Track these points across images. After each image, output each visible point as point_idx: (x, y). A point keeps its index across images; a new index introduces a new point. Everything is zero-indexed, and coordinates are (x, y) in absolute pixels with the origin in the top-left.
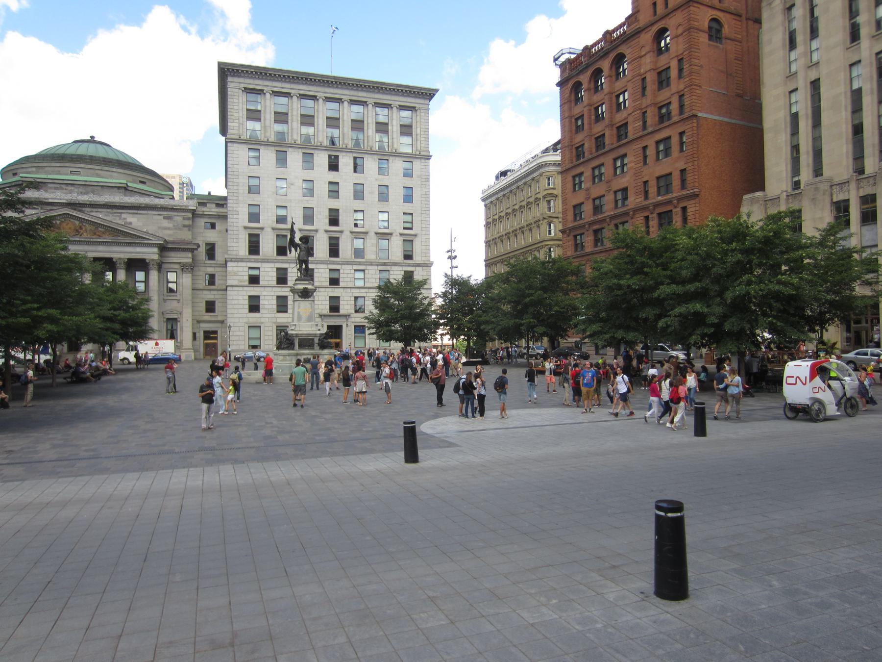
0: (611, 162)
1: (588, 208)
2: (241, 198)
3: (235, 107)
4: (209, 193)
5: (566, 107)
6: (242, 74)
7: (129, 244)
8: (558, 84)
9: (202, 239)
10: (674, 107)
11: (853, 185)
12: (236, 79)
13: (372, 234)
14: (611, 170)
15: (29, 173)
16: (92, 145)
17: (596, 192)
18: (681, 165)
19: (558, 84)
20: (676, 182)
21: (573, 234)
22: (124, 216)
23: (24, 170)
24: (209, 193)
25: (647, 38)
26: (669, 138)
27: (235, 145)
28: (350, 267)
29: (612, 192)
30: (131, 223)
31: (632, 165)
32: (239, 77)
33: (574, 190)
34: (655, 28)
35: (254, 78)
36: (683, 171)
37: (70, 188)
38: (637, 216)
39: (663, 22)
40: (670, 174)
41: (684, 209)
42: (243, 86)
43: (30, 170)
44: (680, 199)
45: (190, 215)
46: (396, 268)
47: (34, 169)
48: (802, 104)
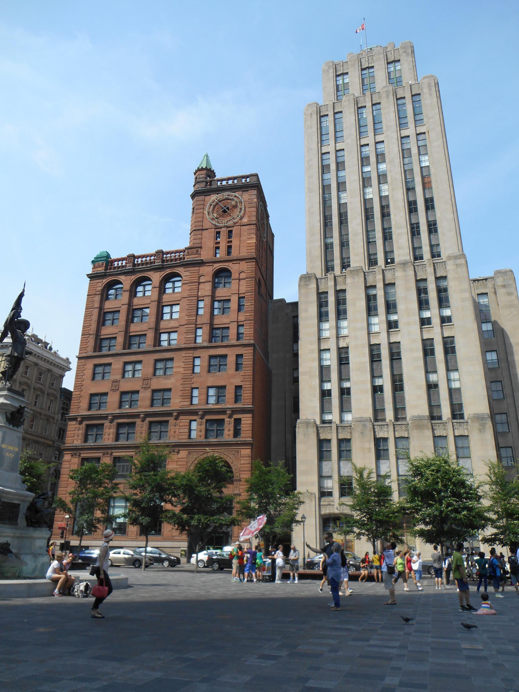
0: (152, 362)
1: (113, 399)
5: (97, 298)
8: (90, 276)
10: (233, 332)
11: (391, 428)
14: (151, 370)
17: (125, 386)
18: (238, 382)
19: (90, 276)
20: (230, 393)
21: (85, 423)
25: (208, 271)
26: (225, 356)
29: (150, 390)
31: (182, 370)
33: (93, 379)
34: (217, 266)
36: (238, 388)
38: (181, 417)
39: (227, 264)
40: (224, 387)
41: (238, 422)
44: (235, 411)
48: (331, 359)
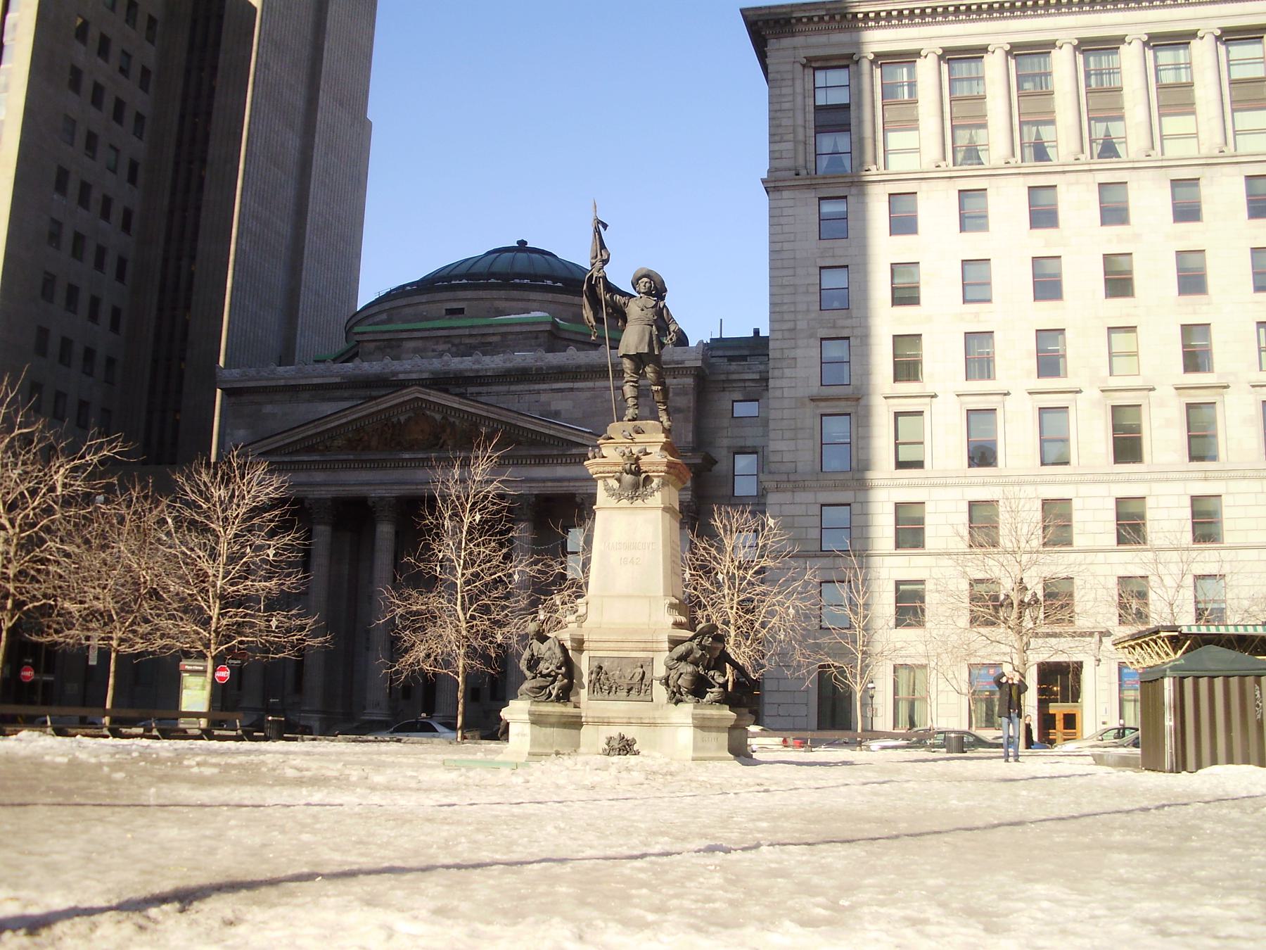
2: (801, 325)
3: (787, 106)
4: (757, 332)
6: (800, 27)
7: (541, 460)
9: (726, 442)
12: (786, 42)
13: (1165, 391)
15: (377, 324)
16: (521, 255)
22: (544, 398)
23: (371, 321)
24: (757, 332)
27: (786, 194)
28: (1101, 489)
30: (557, 414)
32: (793, 34)
35: (829, 31)
37: (441, 347)
42: (802, 55)
43: (377, 319)
45: (689, 381)
46: (1244, 485)
47: (384, 316)
